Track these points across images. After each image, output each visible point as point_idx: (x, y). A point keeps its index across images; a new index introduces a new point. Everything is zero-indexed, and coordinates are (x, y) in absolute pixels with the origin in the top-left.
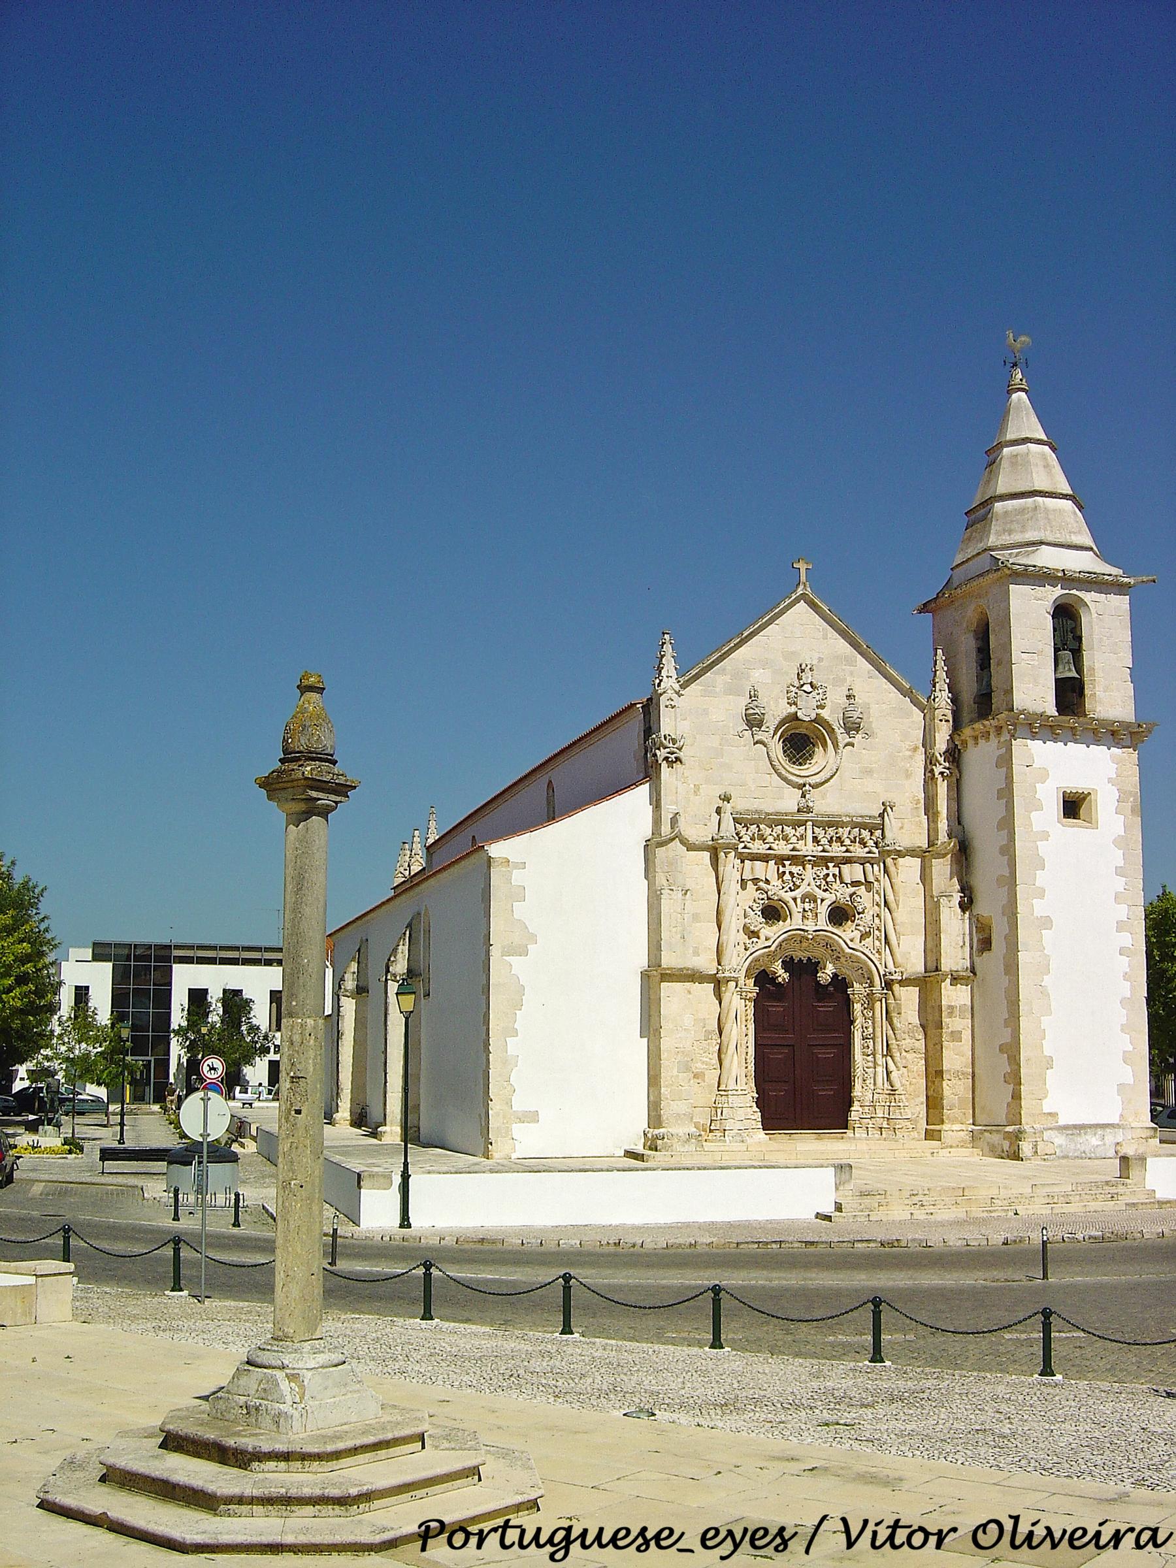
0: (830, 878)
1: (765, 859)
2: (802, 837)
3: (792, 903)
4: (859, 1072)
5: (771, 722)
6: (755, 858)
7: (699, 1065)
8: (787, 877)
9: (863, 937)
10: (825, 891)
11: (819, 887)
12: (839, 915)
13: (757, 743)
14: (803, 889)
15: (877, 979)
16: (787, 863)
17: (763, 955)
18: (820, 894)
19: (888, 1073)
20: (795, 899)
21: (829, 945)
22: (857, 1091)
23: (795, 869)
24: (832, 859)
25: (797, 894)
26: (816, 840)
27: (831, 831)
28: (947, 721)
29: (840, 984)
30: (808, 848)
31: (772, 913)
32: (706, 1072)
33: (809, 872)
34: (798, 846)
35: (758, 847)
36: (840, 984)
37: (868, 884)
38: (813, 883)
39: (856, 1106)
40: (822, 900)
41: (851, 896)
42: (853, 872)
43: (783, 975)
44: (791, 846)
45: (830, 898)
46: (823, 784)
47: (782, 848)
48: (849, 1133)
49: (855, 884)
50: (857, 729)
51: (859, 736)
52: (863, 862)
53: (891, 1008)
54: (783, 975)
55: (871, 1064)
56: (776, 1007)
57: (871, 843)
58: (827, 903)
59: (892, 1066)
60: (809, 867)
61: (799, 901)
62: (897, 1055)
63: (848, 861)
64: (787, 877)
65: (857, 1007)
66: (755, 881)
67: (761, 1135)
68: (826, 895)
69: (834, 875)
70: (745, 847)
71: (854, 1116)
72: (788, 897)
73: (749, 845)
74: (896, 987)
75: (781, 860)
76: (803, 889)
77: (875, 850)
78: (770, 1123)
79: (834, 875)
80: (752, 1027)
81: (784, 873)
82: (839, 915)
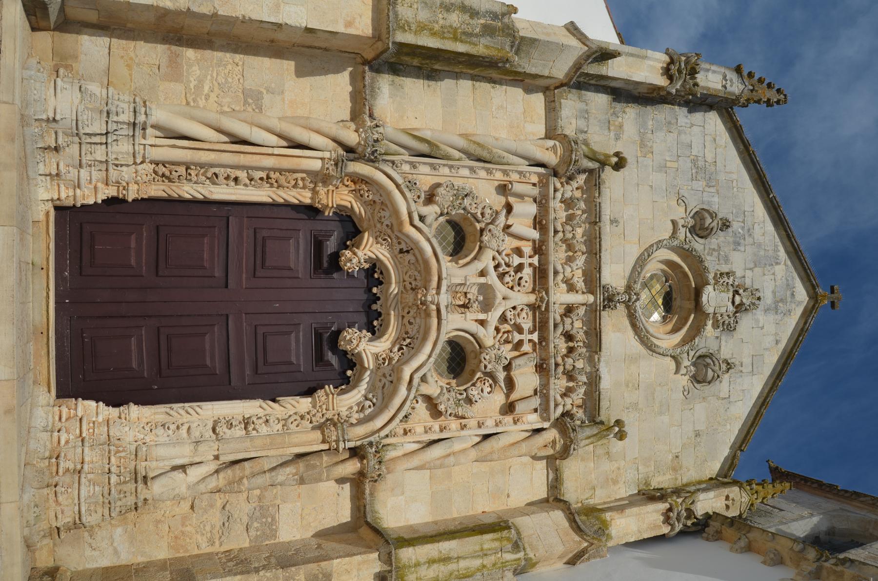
0: (517, 337)
1: (539, 223)
2: (571, 288)
4: (180, 412)
5: (698, 245)
7: (196, 71)
8: (516, 261)
10: (497, 330)
11: (503, 319)
12: (459, 360)
13: (674, 223)
14: (500, 289)
15: (361, 430)
16: (535, 260)
17: (396, 212)
18: (493, 318)
19: (183, 468)
20: (482, 274)
21: (409, 343)
22: (134, 411)
23: (527, 272)
24: (543, 339)
25: (493, 278)
26: (569, 310)
27: (581, 336)
28: (727, 507)
29: (345, 371)
30: (560, 296)
31: (461, 238)
32: (179, 87)
33: (522, 298)
34: (560, 277)
35: (558, 212)
36: (345, 371)
37: (509, 408)
39: (106, 412)
40: (482, 323)
41: (491, 375)
42: (527, 379)
43: (355, 260)
44: (560, 268)
45: (488, 336)
46: (634, 326)
47: (557, 255)
48: (45, 396)
49: (510, 384)
50: (698, 379)
51: (684, 380)
52: (542, 392)
53: (313, 461)
54: (355, 260)
55: (196, 434)
56: (297, 254)
57: (569, 407)
58: (480, 331)
59: (195, 474)
60: (532, 298)
61: (482, 280)
62: (221, 480)
63: (541, 368)
64: (516, 261)
65: (304, 404)
66: (509, 208)
67: (44, 195)
68: (491, 329)
69: (520, 343)
70: (556, 190)
72: (487, 261)
73: (559, 195)
74: (352, 467)
75: (539, 249)
76: (500, 289)
77: (560, 410)
78: (67, 215)
79: (520, 343)
80: (261, 195)
82: (459, 360)
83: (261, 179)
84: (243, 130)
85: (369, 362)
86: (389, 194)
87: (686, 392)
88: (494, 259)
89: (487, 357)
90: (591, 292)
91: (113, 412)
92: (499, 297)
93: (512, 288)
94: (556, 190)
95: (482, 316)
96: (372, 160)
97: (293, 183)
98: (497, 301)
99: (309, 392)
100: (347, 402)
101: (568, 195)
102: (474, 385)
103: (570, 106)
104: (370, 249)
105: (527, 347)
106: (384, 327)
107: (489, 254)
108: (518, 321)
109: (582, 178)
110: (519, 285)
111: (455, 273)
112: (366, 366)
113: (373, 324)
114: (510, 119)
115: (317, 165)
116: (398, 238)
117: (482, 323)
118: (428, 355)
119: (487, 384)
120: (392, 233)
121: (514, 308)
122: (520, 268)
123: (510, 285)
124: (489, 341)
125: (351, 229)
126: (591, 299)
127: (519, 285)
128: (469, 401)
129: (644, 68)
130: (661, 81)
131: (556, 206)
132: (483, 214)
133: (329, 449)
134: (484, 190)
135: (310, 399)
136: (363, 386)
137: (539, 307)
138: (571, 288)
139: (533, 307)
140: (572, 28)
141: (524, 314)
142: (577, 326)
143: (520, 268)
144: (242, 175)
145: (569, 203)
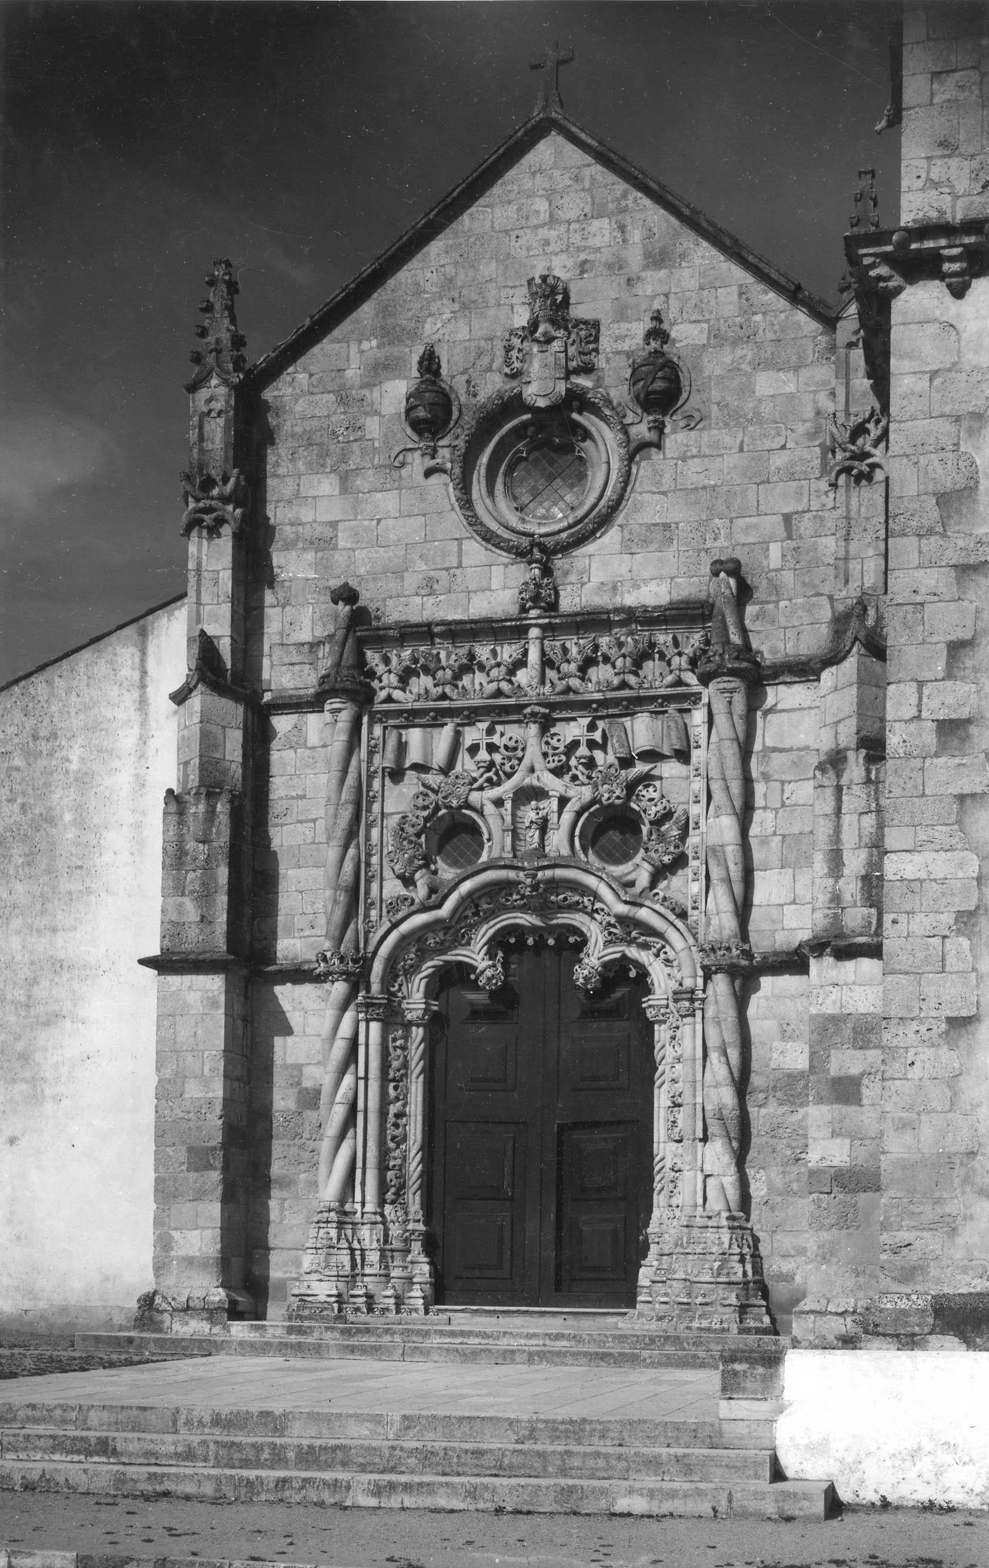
3: (489, 809)
6: (411, 717)
8: (483, 755)
9: (660, 873)
11: (559, 772)
12: (612, 828)
13: (428, 473)
18: (555, 785)
20: (499, 803)
25: (506, 790)
29: (625, 982)
38: (539, 764)
40: (563, 801)
41: (631, 788)
42: (642, 731)
57: (684, 661)
64: (483, 755)
65: (661, 1033)
71: (645, 1275)
81: (474, 749)
82: (612, 828)
83: (396, 1088)
84: (339, 1112)
85: (614, 952)
86: (404, 938)
87: (692, 423)
88: (481, 788)
89: (606, 796)
90: (525, 629)
91: (654, 1249)
92: (530, 780)
93: (520, 760)
94: (389, 699)
95: (555, 804)
96: (366, 963)
97: (399, 1051)
98: (535, 783)
99: (648, 1027)
100: (662, 981)
101: (393, 679)
102: (645, 811)
103: (282, 674)
104: (475, 954)
105: (597, 736)
106: (575, 930)
107: (475, 797)
108: (562, 749)
109: (373, 657)
110: (515, 749)
111: (496, 844)
112: (618, 955)
113: (573, 945)
114: (307, 758)
115: (375, 1027)
116: (460, 919)
117: (563, 801)
118: (599, 880)
119: (644, 793)
120: (455, 930)
121: (545, 755)
122: (492, 748)
123: (516, 762)
124: (586, 793)
125: (453, 978)
126: (534, 632)
127: (515, 749)
128: (668, 815)
129: (213, 559)
130: (225, 544)
131: (406, 699)
132: (425, 808)
133: (703, 1010)
134: (399, 800)
135: (656, 1027)
136: (644, 957)
137: (544, 716)
138: (521, 663)
139: (546, 724)
140: (180, 697)
141: (554, 742)
142: (575, 646)
143: (492, 748)
144: (393, 1109)
145: (405, 677)
